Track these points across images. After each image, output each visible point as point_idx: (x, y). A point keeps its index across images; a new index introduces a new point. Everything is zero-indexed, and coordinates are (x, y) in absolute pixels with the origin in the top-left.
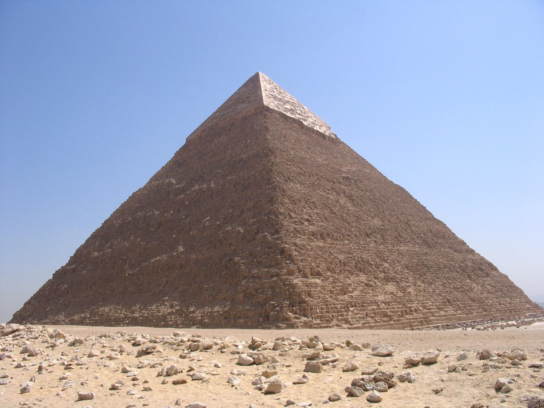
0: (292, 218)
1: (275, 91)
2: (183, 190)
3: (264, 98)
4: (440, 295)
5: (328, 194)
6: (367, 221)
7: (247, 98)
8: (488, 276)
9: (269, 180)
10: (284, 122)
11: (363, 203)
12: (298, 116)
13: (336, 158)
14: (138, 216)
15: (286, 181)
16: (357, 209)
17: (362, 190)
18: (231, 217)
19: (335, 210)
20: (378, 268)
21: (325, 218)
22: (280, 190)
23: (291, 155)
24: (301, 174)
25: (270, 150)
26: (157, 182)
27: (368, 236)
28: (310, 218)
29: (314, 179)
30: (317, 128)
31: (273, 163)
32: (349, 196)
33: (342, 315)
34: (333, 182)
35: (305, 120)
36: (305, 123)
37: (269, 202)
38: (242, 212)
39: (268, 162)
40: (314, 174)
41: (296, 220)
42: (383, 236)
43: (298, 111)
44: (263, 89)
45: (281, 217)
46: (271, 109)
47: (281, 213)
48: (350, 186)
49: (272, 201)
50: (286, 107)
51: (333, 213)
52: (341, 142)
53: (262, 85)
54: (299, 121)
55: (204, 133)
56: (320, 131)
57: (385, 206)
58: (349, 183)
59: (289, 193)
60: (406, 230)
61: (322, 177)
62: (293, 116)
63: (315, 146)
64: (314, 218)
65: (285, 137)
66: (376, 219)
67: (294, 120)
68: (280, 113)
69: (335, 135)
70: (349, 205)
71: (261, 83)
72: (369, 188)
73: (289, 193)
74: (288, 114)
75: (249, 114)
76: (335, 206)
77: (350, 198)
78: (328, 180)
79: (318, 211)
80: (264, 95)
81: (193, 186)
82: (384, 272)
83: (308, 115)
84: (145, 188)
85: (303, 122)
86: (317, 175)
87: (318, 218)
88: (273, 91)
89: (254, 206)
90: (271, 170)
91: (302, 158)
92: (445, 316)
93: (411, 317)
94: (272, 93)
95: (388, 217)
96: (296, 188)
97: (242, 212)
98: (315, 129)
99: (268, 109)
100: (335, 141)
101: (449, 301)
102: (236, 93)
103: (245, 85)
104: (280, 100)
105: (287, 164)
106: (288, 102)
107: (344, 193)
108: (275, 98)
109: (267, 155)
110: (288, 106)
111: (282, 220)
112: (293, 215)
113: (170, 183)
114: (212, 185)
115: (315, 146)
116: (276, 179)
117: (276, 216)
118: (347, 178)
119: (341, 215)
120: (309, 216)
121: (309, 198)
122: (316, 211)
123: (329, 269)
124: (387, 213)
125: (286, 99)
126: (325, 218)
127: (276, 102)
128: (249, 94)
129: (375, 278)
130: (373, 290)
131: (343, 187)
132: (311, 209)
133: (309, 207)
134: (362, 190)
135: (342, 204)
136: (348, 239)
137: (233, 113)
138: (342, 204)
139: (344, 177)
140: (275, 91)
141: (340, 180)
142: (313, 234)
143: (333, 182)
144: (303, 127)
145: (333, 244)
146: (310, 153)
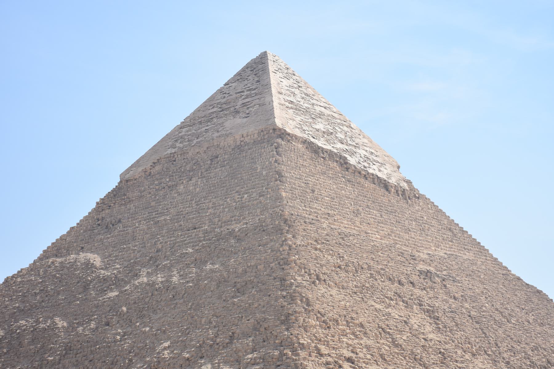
0: (321, 355)
1: (297, 91)
2: (117, 282)
3: (277, 112)
5: (390, 305)
6: (462, 362)
7: (244, 105)
9: (283, 280)
10: (311, 159)
11: (457, 325)
12: (339, 145)
13: (408, 231)
14: (19, 327)
15: (314, 283)
16: (442, 338)
17: (455, 298)
18: (211, 346)
19: (401, 339)
21: (382, 356)
22: (301, 300)
23: (324, 229)
24: (339, 267)
25: (286, 221)
26: (59, 260)
28: (353, 356)
29: (363, 277)
30: (373, 170)
31: (290, 246)
32: (428, 311)
34: (400, 283)
35: (353, 154)
36: (352, 161)
37: (283, 323)
38: (232, 338)
39: (282, 245)
40: (365, 266)
41: (330, 359)
43: (341, 136)
44: (274, 91)
45: (303, 354)
46: (289, 134)
47: (303, 347)
48: (432, 288)
49: (287, 320)
50: (317, 127)
51: (397, 346)
52: (419, 197)
53: (272, 81)
54: (341, 157)
55: (158, 168)
56: (380, 175)
57: (500, 331)
58: (430, 284)
59: (317, 307)
61: (379, 273)
62: (328, 147)
63: (368, 206)
64: (361, 355)
65: (313, 191)
66: (480, 359)
67: (331, 155)
68: (305, 142)
69: (409, 182)
70: (428, 328)
71: (272, 75)
72: (469, 293)
73: (317, 307)
74: (321, 143)
75: (247, 140)
76: (401, 332)
77: (431, 313)
78: (390, 279)
79: (369, 342)
80: (275, 104)
81: (137, 276)
83: (357, 141)
84: (33, 268)
85: (349, 158)
86: (369, 268)
87: (369, 357)
88: (294, 94)
89: (255, 329)
90: (287, 263)
91: (344, 236)
94: (292, 99)
95: (505, 355)
96: (329, 297)
97: (232, 338)
98: (371, 171)
99: (283, 134)
100: (408, 194)
102: (220, 91)
103: (240, 77)
104: (306, 111)
105: (316, 249)
106: (321, 115)
107: (421, 305)
108: (297, 109)
109: (279, 230)
110: (320, 126)
111: (304, 359)
112: (324, 350)
113: (88, 265)
114: (175, 279)
115: (368, 206)
116: (295, 280)
117: (294, 351)
118: (427, 274)
119: (413, 353)
120: (353, 352)
121: (354, 316)
122: (365, 341)
124: (504, 346)
125: (318, 109)
126: (382, 356)
127: (298, 118)
128: (247, 97)
131: (417, 292)
132: (356, 337)
133: (354, 334)
134: (455, 298)
135: (416, 326)
137: (216, 134)
138: (416, 326)
139: (421, 272)
140: (297, 91)
141: (415, 278)
143: (400, 283)
144: (347, 169)
146: (358, 223)
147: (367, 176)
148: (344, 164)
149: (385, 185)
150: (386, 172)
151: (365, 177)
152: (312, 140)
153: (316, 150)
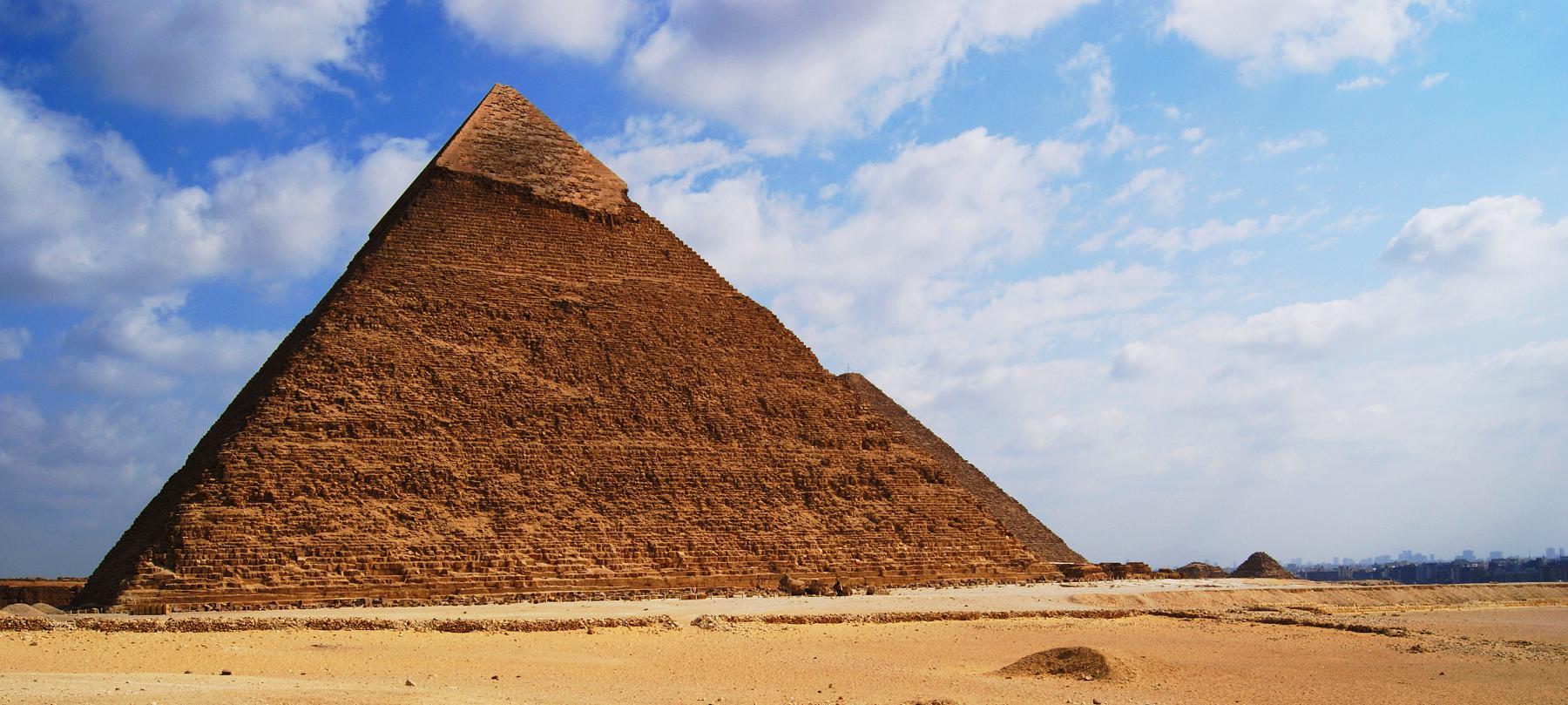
4: (630, 535)
8: (887, 495)
17: (592, 327)
19: (444, 376)
20: (477, 485)
27: (510, 423)
33: (263, 569)
35: (544, 183)
36: (539, 190)
42: (557, 421)
47: (279, 392)
56: (578, 202)
58: (560, 313)
60: (667, 404)
67: (511, 188)
68: (473, 178)
82: (485, 493)
92: (596, 576)
93: (476, 575)
101: (651, 548)
118: (564, 305)
119: (455, 388)
123: (306, 490)
125: (531, 138)
129: (447, 504)
130: (409, 526)
132: (377, 377)
136: (434, 432)
142: (329, 426)
143: (506, 317)
145: (373, 442)
147: (558, 205)
148: (526, 193)
149: (582, 213)
150: (592, 197)
151: (556, 207)
152: (487, 174)
153: (487, 185)
